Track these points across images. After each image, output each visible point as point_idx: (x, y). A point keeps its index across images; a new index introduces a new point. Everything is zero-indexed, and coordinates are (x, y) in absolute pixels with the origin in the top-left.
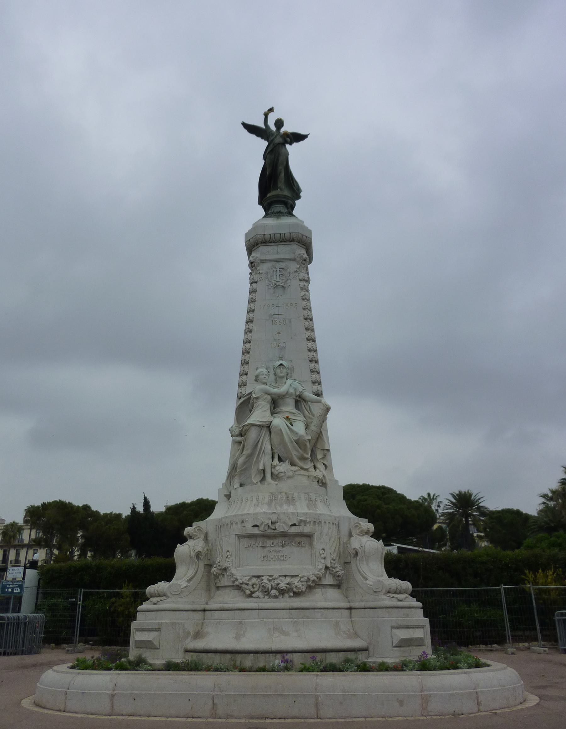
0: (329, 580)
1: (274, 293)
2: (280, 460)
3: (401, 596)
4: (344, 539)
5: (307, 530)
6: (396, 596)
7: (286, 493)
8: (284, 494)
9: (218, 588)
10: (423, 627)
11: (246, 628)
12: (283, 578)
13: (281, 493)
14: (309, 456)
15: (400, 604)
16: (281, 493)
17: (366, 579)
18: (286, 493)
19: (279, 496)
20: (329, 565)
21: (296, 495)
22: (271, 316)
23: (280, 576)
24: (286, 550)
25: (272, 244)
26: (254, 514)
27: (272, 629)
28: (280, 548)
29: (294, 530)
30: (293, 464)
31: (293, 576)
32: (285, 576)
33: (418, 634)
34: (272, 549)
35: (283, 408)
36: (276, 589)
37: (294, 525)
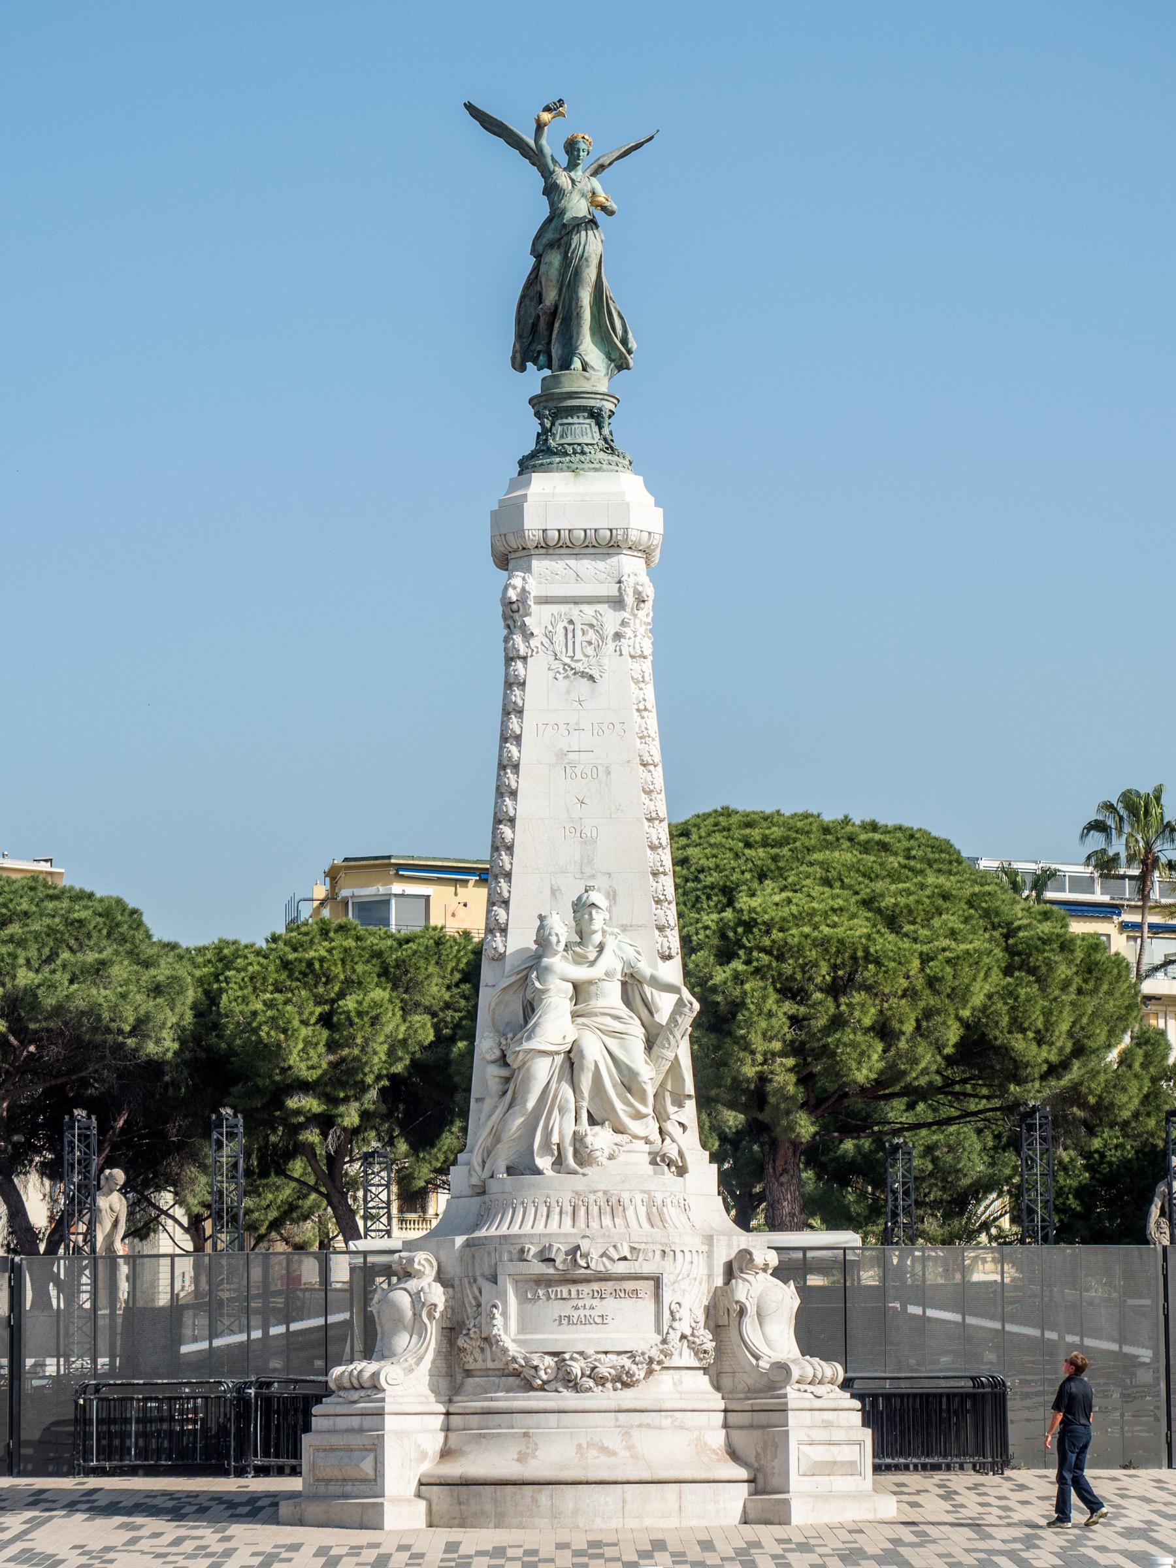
0: (688, 1359)
1: (568, 692)
2: (592, 1121)
3: (820, 1390)
4: (719, 1281)
5: (647, 1268)
6: (810, 1388)
7: (605, 1192)
8: (600, 1194)
9: (468, 1373)
10: (860, 1443)
11: (536, 1444)
12: (602, 1356)
13: (596, 1192)
14: (648, 1110)
15: (818, 1403)
16: (596, 1192)
17: (757, 1358)
18: (605, 1192)
19: (592, 1197)
20: (688, 1332)
21: (625, 1196)
22: (561, 754)
23: (598, 1353)
24: (609, 1305)
25: (563, 551)
26: (545, 1235)
27: (585, 1446)
28: (595, 1302)
29: (621, 1268)
30: (616, 1131)
31: (619, 1353)
32: (606, 1353)
33: (849, 1454)
34: (580, 1303)
35: (598, 1004)
36: (589, 1376)
37: (625, 1259)
